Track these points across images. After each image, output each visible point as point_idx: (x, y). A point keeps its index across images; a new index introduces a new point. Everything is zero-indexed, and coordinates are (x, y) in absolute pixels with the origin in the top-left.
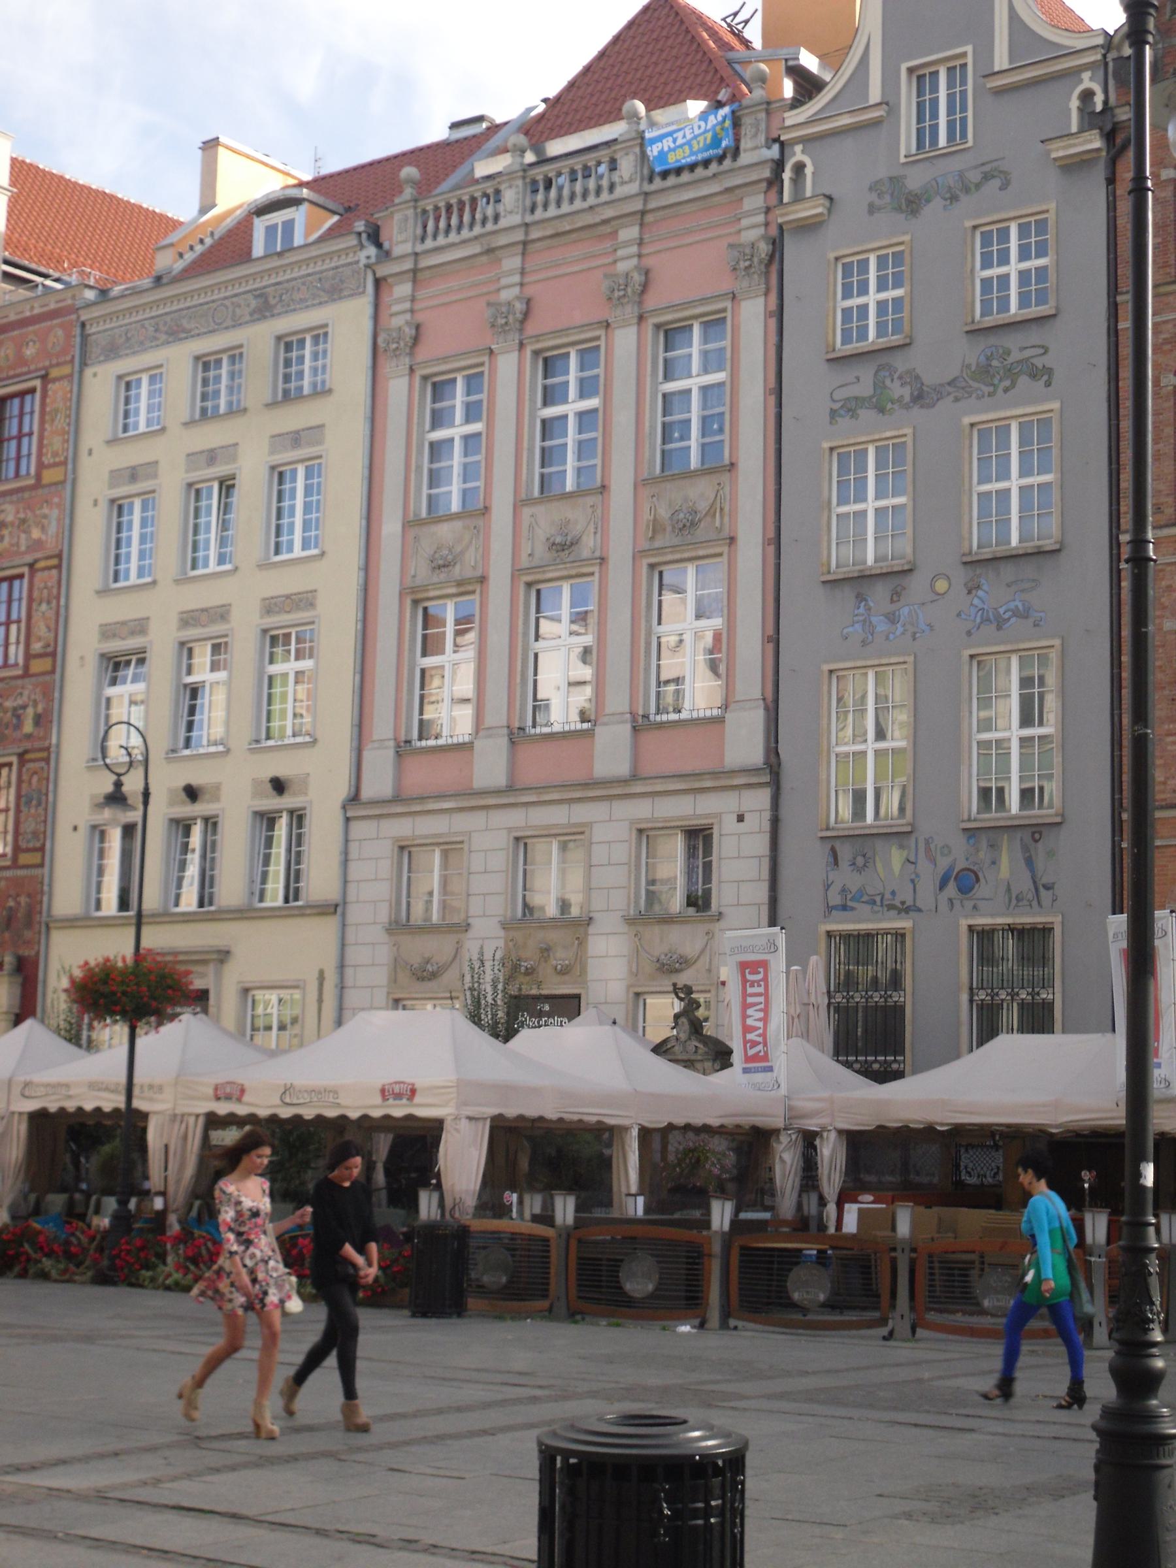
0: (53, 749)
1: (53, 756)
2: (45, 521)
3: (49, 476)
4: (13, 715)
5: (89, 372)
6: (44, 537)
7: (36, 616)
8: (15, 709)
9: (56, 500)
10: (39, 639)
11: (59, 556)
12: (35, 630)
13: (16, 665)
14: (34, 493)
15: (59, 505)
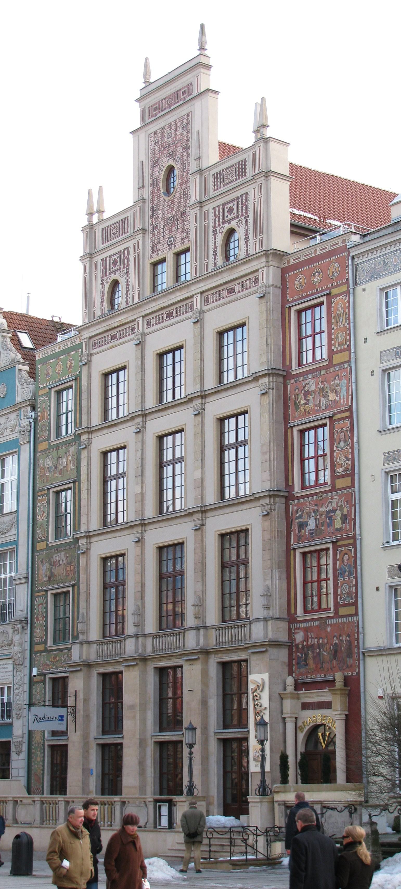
0: (358, 536)
1: (358, 542)
2: (338, 389)
3: (337, 359)
4: (326, 517)
5: (359, 289)
6: (338, 399)
7: (337, 451)
8: (327, 513)
9: (344, 374)
10: (341, 465)
11: (350, 410)
12: (337, 460)
13: (325, 483)
14: (328, 371)
15: (346, 377)
